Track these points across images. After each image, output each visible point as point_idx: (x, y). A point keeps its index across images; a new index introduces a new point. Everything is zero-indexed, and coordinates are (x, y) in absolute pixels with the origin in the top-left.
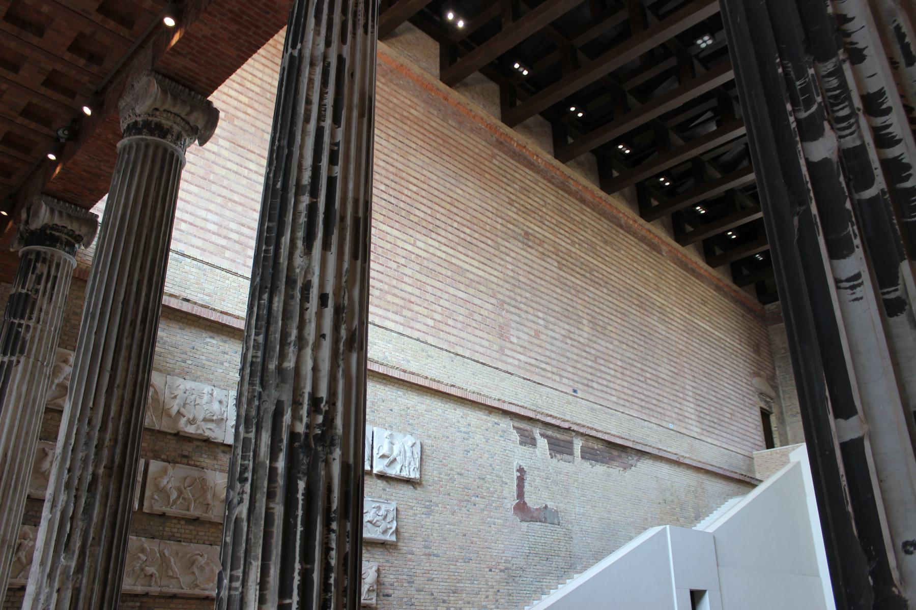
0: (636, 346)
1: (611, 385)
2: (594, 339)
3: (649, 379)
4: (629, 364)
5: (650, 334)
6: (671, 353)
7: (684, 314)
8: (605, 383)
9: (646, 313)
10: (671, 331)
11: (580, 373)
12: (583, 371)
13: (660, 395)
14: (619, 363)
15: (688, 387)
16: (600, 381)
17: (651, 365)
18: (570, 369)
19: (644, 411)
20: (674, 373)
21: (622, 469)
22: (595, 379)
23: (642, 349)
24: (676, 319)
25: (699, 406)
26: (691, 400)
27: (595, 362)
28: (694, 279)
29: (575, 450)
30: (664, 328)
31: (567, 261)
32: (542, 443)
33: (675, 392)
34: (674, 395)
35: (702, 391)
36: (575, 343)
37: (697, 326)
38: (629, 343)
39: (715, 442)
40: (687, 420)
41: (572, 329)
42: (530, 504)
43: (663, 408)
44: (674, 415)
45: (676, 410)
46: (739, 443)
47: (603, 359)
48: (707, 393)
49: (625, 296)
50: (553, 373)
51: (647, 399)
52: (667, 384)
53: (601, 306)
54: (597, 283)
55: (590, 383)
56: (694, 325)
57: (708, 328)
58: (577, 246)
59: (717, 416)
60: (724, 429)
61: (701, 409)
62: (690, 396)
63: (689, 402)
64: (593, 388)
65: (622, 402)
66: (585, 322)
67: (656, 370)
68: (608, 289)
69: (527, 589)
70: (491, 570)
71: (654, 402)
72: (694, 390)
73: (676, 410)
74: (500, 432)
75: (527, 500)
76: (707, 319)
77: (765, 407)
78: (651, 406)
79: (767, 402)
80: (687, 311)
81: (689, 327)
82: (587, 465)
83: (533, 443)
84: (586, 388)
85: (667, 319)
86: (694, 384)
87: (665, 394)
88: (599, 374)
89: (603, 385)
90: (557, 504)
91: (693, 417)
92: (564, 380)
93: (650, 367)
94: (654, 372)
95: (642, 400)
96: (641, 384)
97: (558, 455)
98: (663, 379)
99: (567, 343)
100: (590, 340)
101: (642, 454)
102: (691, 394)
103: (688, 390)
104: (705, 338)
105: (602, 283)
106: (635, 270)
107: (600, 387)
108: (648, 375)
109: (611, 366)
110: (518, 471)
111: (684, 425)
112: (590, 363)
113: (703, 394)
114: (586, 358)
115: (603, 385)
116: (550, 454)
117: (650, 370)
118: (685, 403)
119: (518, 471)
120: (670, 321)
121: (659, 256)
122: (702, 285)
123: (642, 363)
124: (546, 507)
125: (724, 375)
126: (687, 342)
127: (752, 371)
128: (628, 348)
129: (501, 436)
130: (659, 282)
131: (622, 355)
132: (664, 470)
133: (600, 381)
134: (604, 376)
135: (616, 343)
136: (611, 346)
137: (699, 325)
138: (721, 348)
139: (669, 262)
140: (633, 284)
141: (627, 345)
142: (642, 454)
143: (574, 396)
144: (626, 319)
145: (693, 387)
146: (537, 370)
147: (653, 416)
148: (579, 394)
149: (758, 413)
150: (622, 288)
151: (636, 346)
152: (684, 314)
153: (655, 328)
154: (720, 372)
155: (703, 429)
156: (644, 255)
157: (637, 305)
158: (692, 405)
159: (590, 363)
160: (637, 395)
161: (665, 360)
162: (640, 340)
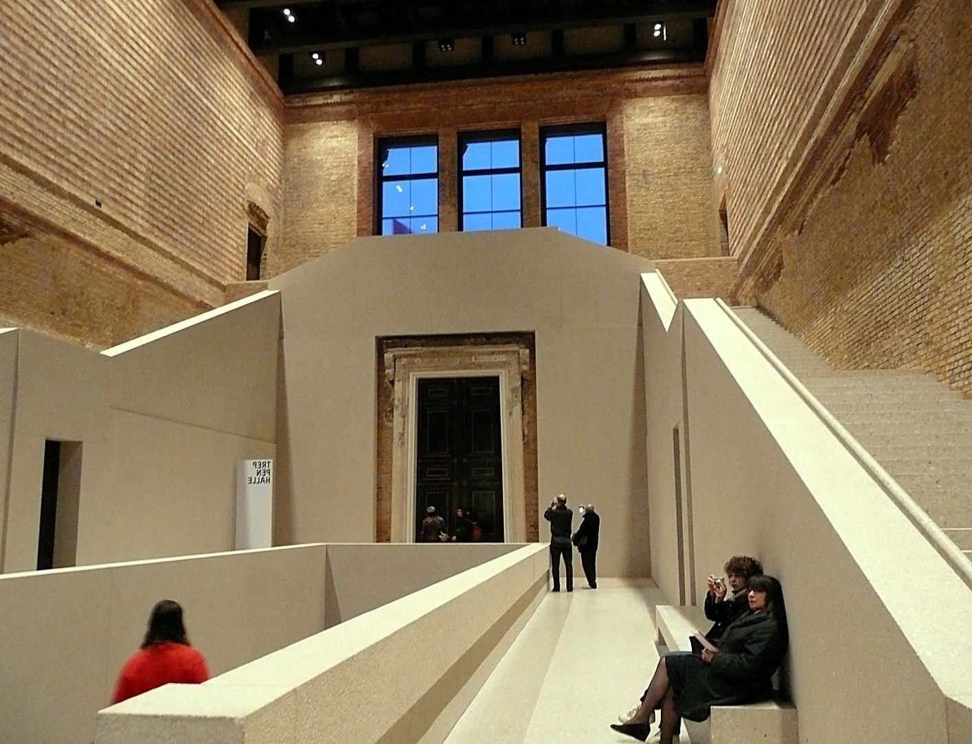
3: (72, 121)
5: (89, 55)
13: (87, 153)
15: (140, 157)
23: (68, 71)
25: (154, 191)
26: (143, 178)
28: (186, 10)
34: (113, 161)
38: (42, 50)
44: (107, 191)
45: (112, 185)
46: (208, 260)
52: (103, 140)
57: (193, 88)
59: (181, 214)
62: (142, 172)
63: (138, 179)
76: (196, 75)
77: (256, 226)
80: (164, 50)
86: (152, 158)
87: (96, 155)
91: (140, 203)
93: (77, 104)
95: (51, 150)
96: (52, 123)
98: (99, 131)
103: (140, 163)
104: (184, 100)
111: (123, 211)
113: (165, 178)
117: (76, 109)
118: (131, 178)
120: (129, 50)
123: (62, 93)
126: (152, 94)
141: (38, 53)
145: (149, 161)
147: (67, 180)
152: (158, 51)
155: (154, 225)
158: (142, 186)
160: (40, 137)
161: (109, 106)
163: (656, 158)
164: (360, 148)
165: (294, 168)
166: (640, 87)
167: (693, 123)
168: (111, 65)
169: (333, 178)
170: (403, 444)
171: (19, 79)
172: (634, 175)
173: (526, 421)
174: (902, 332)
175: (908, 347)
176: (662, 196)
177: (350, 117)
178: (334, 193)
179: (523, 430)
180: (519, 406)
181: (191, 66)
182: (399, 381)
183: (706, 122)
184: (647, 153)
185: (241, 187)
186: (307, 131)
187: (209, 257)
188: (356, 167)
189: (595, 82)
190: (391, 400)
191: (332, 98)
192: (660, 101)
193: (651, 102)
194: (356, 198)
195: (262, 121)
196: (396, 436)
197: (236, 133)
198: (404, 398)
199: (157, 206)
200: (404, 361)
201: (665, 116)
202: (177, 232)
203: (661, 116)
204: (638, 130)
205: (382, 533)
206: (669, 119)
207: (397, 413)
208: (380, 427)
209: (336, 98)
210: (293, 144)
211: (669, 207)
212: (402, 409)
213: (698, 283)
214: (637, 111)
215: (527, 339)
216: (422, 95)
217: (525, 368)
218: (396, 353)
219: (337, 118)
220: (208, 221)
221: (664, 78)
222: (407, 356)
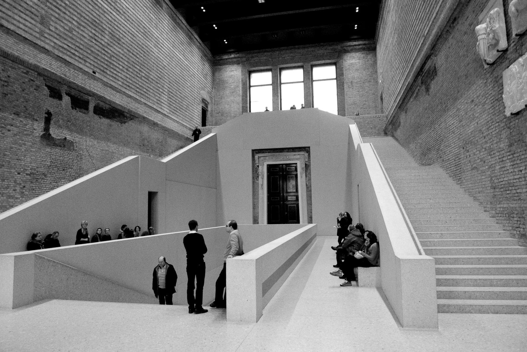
0: (138, 56)
3: (143, 77)
5: (148, 52)
6: (159, 66)
7: (170, 46)
9: (147, 39)
11: (99, 62)
13: (149, 87)
14: (126, 63)
15: (165, 87)
18: (92, 58)
20: (159, 77)
23: (142, 59)
25: (170, 98)
26: (166, 94)
27: (110, 58)
28: (179, 29)
32: (66, 99)
34: (157, 89)
37: (176, 55)
38: (134, 53)
40: (162, 104)
42: (53, 136)
43: (149, 95)
44: (155, 100)
45: (157, 98)
46: (189, 122)
48: (175, 92)
49: (136, 25)
50: (80, 58)
52: (154, 82)
53: (119, 26)
54: (118, 11)
55: (105, 70)
56: (174, 54)
57: (182, 58)
59: (179, 105)
60: (181, 113)
62: (166, 92)
63: (165, 94)
64: (106, 73)
68: (125, 17)
69: (47, 186)
70: (19, 174)
71: (145, 90)
72: (169, 89)
74: (35, 87)
75: (51, 132)
76: (182, 53)
77: (204, 106)
78: (143, 93)
80: (172, 45)
81: (171, 54)
82: (96, 117)
83: (60, 98)
84: (102, 73)
86: (169, 86)
87: (152, 88)
90: (74, 138)
91: (166, 103)
92: (87, 64)
93: (145, 70)
95: (138, 88)
96: (138, 78)
97: (78, 109)
98: (152, 79)
102: (166, 91)
103: (166, 88)
104: (179, 63)
105: (122, 13)
106: (144, 12)
109: (121, 63)
110: (46, 113)
111: (160, 106)
116: (72, 107)
117: (145, 72)
118: (163, 95)
119: (46, 113)
120: (161, 48)
121: (160, 8)
122: (183, 33)
123: (140, 67)
124: (65, 138)
126: (169, 62)
129: (35, 89)
130: (158, 24)
139: (166, 14)
140: (142, 19)
141: (133, 54)
145: (168, 87)
146: (68, 53)
147: (143, 98)
148: (97, 75)
149: (201, 109)
150: (134, 20)
152: (170, 46)
153: (151, 49)
154: (185, 83)
155: (170, 111)
156: (151, 5)
157: (143, 33)
158: (166, 97)
160: (134, 84)
162: (142, 53)
163: (356, 76)
164: (242, 75)
165: (217, 83)
166: (349, 48)
167: (370, 62)
168: (155, 54)
169: (232, 87)
170: (262, 188)
171: (127, 64)
172: (347, 83)
174: (434, 152)
176: (358, 91)
177: (238, 64)
178: (233, 92)
180: (304, 174)
181: (180, 50)
183: (375, 62)
184: (352, 74)
185: (199, 93)
186: (222, 69)
187: (189, 120)
188: (241, 83)
189: (332, 47)
191: (231, 56)
192: (357, 54)
193: (353, 54)
194: (241, 94)
195: (205, 67)
196: (260, 186)
197: (197, 72)
198: (262, 172)
199: (171, 104)
200: (262, 158)
201: (359, 60)
202: (178, 112)
203: (358, 60)
204: (349, 65)
205: (256, 221)
206: (361, 61)
207: (260, 177)
208: (254, 182)
209: (233, 56)
210: (217, 74)
211: (361, 95)
212: (262, 176)
213: (371, 126)
214: (349, 58)
215: (306, 149)
216: (265, 54)
217: (307, 160)
218: (259, 156)
219: (233, 63)
220: (188, 107)
221: (359, 45)
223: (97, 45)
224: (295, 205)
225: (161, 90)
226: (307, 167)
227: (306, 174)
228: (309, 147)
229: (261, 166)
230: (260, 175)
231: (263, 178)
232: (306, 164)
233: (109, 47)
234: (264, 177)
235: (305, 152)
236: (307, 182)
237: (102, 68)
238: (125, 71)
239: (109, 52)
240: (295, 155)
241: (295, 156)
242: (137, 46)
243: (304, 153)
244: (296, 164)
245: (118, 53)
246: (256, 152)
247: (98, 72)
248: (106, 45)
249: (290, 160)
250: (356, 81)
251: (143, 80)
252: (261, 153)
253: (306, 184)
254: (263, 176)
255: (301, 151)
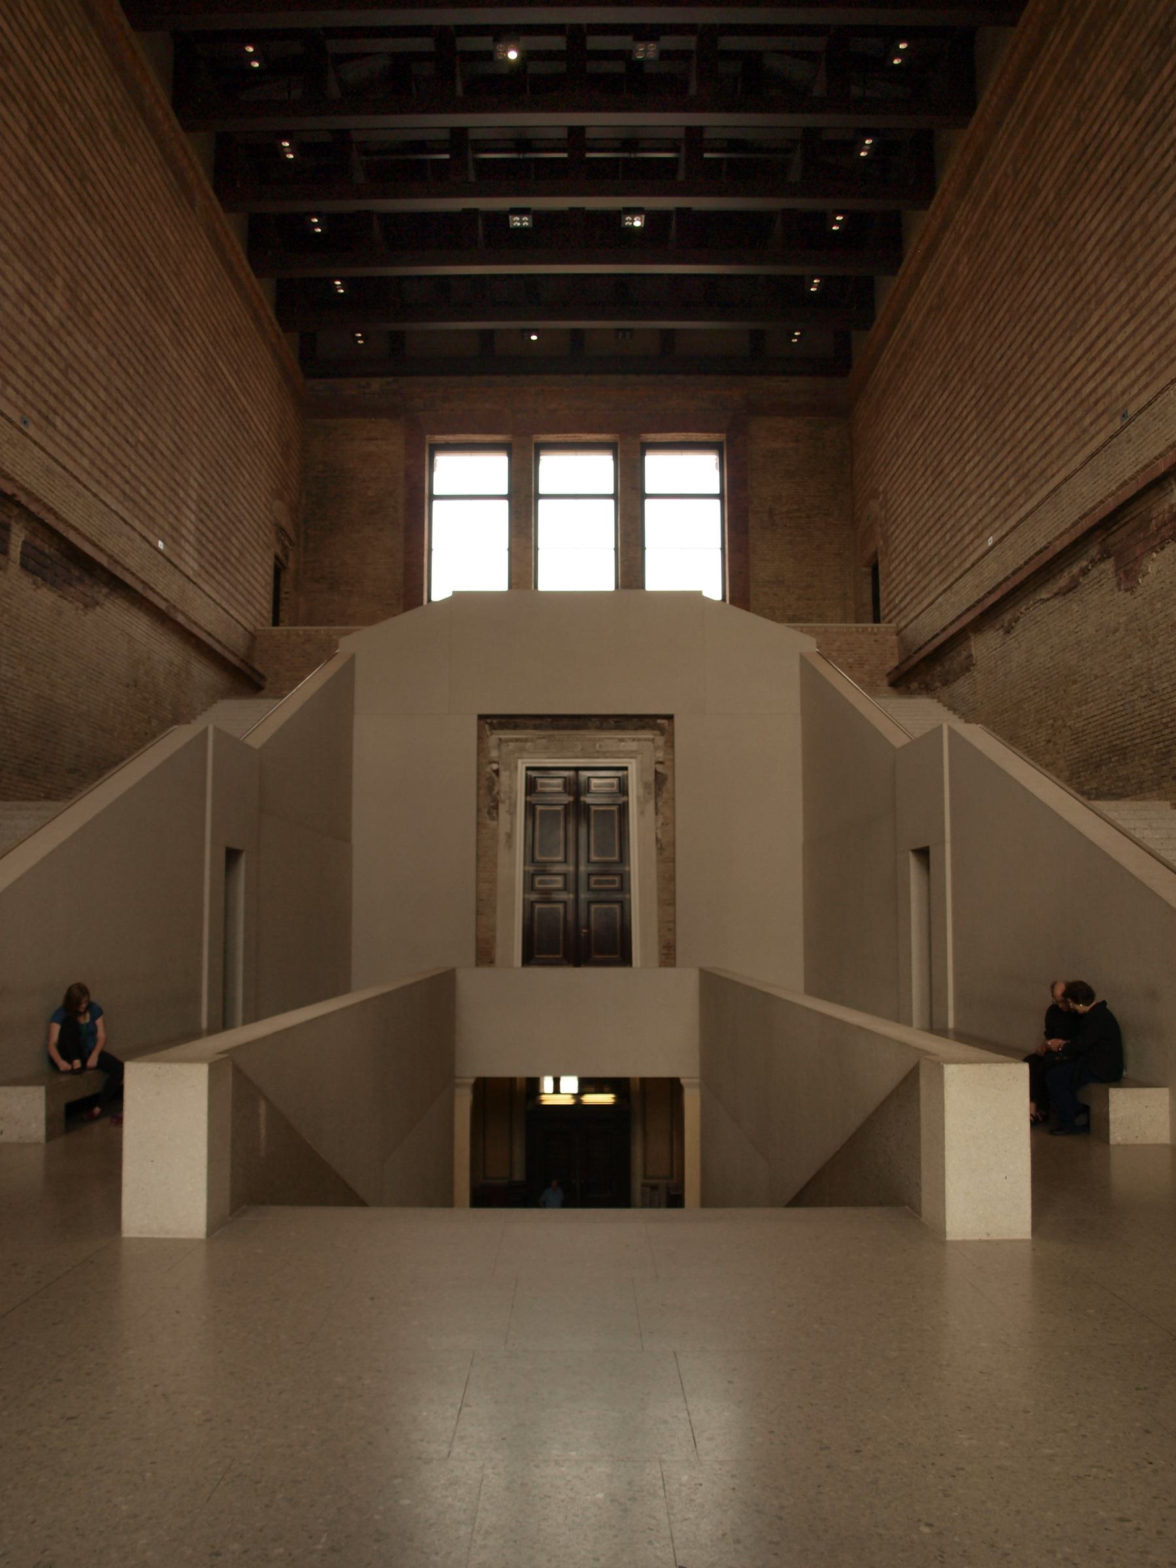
0: (131, 371)
1: (85, 433)
2: (69, 325)
3: (142, 444)
4: (117, 402)
6: (179, 408)
8: (75, 424)
10: (183, 365)
11: (37, 386)
12: (44, 385)
14: (102, 394)
15: (192, 481)
16: (68, 416)
17: (149, 419)
18: (22, 371)
19: (126, 504)
20: (178, 448)
21: (81, 606)
22: (61, 410)
24: (194, 346)
27: (64, 373)
29: (12, 547)
30: (175, 354)
31: (46, 131)
33: (173, 484)
35: (210, 496)
36: (36, 320)
37: (220, 374)
39: (214, 595)
40: (183, 542)
41: (36, 287)
43: (154, 508)
44: (167, 527)
47: (79, 375)
51: (134, 483)
53: (89, 261)
55: (51, 416)
58: (67, 107)
60: (228, 575)
61: (204, 530)
64: (54, 426)
65: (96, 473)
66: (59, 282)
67: (154, 432)
71: (143, 491)
72: (200, 491)
73: (171, 519)
78: (138, 498)
79: (285, 548)
80: (212, 339)
82: (26, 581)
84: (44, 423)
85: (182, 340)
88: (68, 403)
89: (70, 426)
94: (151, 435)
99: (22, 312)
100: (62, 325)
101: (117, 585)
102: (194, 495)
103: (192, 487)
105: (98, 217)
106: (151, 217)
107: (66, 430)
108: (142, 438)
112: (56, 373)
113: (211, 503)
114: (50, 360)
115: (70, 426)
117: (146, 429)
125: (241, 479)
127: (274, 487)
128: (118, 369)
131: (109, 379)
132: (140, 626)
133: (68, 416)
134: (75, 409)
135: (103, 351)
136: (93, 353)
137: (223, 374)
138: (245, 429)
141: (119, 362)
142: (117, 585)
143: (21, 430)
144: (125, 309)
149: (271, 562)
151: (131, 371)
152: (207, 342)
159: (56, 373)
161: (170, 419)
168: (171, 366)
169: (370, 493)
171: (104, 399)
173: (659, 824)
174: (1144, 761)
175: (1150, 777)
179: (656, 834)
180: (651, 806)
182: (506, 770)
190: (494, 793)
196: (502, 838)
197: (266, 436)
198: (512, 790)
200: (512, 745)
205: (485, 956)
207: (503, 809)
213: (851, 660)
218: (503, 737)
222: (517, 740)
223: (34, 325)
224: (616, 906)
225: (182, 494)
226: (660, 782)
227: (656, 804)
228: (670, 718)
229: (507, 773)
230: (503, 802)
231: (512, 813)
232: (656, 772)
233: (63, 333)
234: (515, 806)
235: (657, 732)
236: (659, 831)
237: (44, 409)
238: (99, 420)
239: (65, 352)
240: (622, 740)
241: (623, 744)
242: (131, 338)
243: (652, 737)
244: (626, 769)
245: (82, 355)
246: (491, 725)
247: (34, 422)
248: (56, 325)
249: (605, 755)
250: (784, 509)
251: (141, 457)
252: (508, 728)
253: (657, 838)
254: (513, 806)
255: (643, 728)
